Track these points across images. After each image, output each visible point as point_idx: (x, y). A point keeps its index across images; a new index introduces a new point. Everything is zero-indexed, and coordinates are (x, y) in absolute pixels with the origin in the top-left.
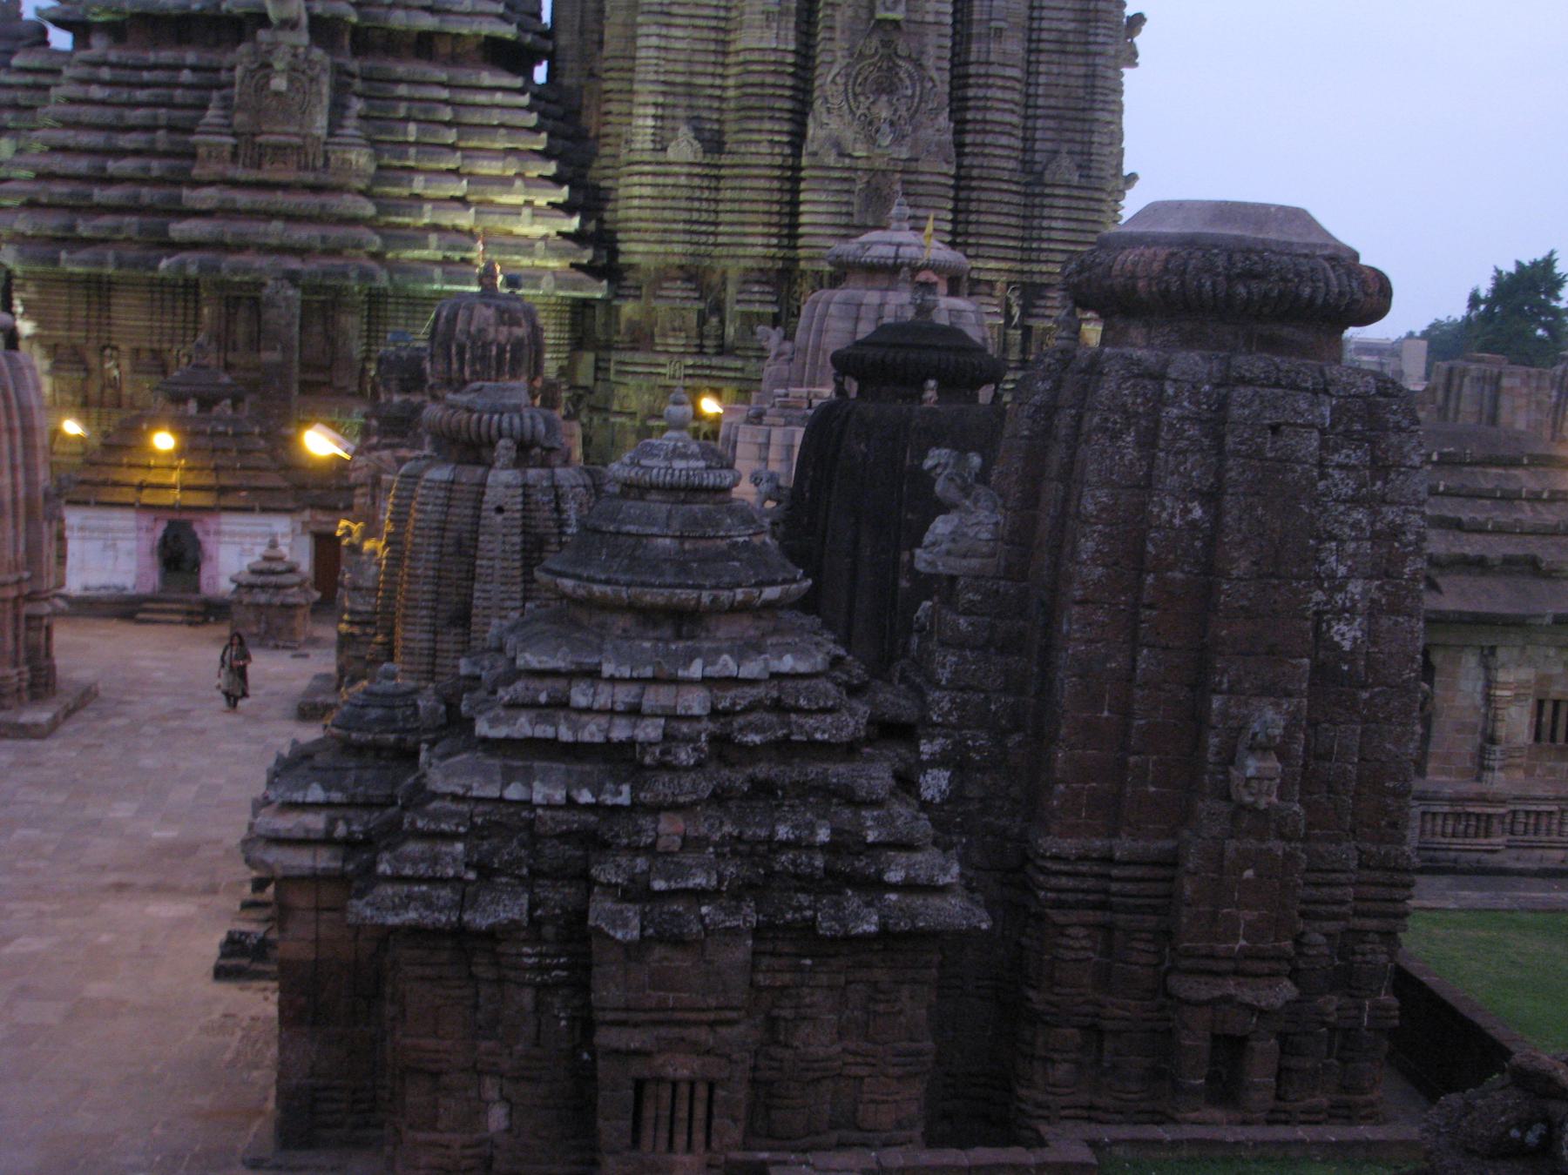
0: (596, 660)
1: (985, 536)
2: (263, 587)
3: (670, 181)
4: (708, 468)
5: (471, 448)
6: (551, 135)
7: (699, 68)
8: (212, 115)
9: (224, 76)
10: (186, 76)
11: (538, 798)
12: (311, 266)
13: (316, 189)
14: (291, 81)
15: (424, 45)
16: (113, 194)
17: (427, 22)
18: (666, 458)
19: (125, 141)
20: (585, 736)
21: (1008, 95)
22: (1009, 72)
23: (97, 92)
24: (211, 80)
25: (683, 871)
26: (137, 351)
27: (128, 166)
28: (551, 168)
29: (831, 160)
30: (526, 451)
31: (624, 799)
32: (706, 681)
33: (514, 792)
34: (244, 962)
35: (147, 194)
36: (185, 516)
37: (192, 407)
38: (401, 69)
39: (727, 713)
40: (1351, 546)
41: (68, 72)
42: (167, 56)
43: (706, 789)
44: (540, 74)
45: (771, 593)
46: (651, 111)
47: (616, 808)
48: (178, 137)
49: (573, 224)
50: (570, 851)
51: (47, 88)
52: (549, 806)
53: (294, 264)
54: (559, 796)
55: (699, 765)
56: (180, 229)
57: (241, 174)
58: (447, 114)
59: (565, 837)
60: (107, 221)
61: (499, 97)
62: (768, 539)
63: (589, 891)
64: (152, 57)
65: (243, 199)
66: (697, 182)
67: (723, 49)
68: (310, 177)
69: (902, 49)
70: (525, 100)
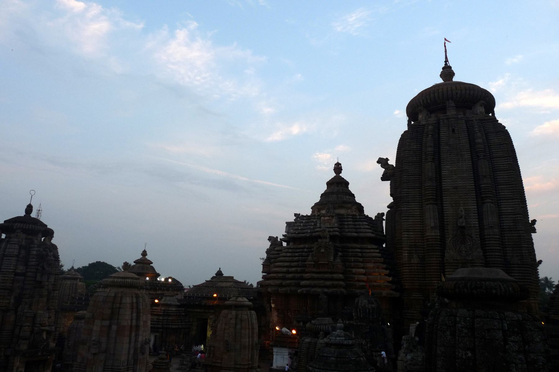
1: (420, 360)
3: (413, 268)
4: (345, 339)
7: (417, 241)
8: (310, 258)
9: (312, 249)
10: (305, 250)
12: (330, 290)
13: (331, 273)
15: (356, 240)
16: (290, 276)
17: (355, 234)
18: (336, 337)
19: (293, 264)
21: (496, 242)
22: (496, 237)
23: (289, 254)
27: (293, 269)
28: (385, 266)
35: (298, 275)
38: (350, 245)
40: (520, 366)
41: (283, 251)
42: (302, 246)
44: (384, 246)
46: (406, 252)
49: (390, 279)
53: (326, 290)
56: (303, 283)
58: (360, 254)
60: (288, 282)
61: (372, 251)
62: (362, 359)
65: (315, 276)
66: (419, 268)
68: (330, 270)
70: (378, 251)
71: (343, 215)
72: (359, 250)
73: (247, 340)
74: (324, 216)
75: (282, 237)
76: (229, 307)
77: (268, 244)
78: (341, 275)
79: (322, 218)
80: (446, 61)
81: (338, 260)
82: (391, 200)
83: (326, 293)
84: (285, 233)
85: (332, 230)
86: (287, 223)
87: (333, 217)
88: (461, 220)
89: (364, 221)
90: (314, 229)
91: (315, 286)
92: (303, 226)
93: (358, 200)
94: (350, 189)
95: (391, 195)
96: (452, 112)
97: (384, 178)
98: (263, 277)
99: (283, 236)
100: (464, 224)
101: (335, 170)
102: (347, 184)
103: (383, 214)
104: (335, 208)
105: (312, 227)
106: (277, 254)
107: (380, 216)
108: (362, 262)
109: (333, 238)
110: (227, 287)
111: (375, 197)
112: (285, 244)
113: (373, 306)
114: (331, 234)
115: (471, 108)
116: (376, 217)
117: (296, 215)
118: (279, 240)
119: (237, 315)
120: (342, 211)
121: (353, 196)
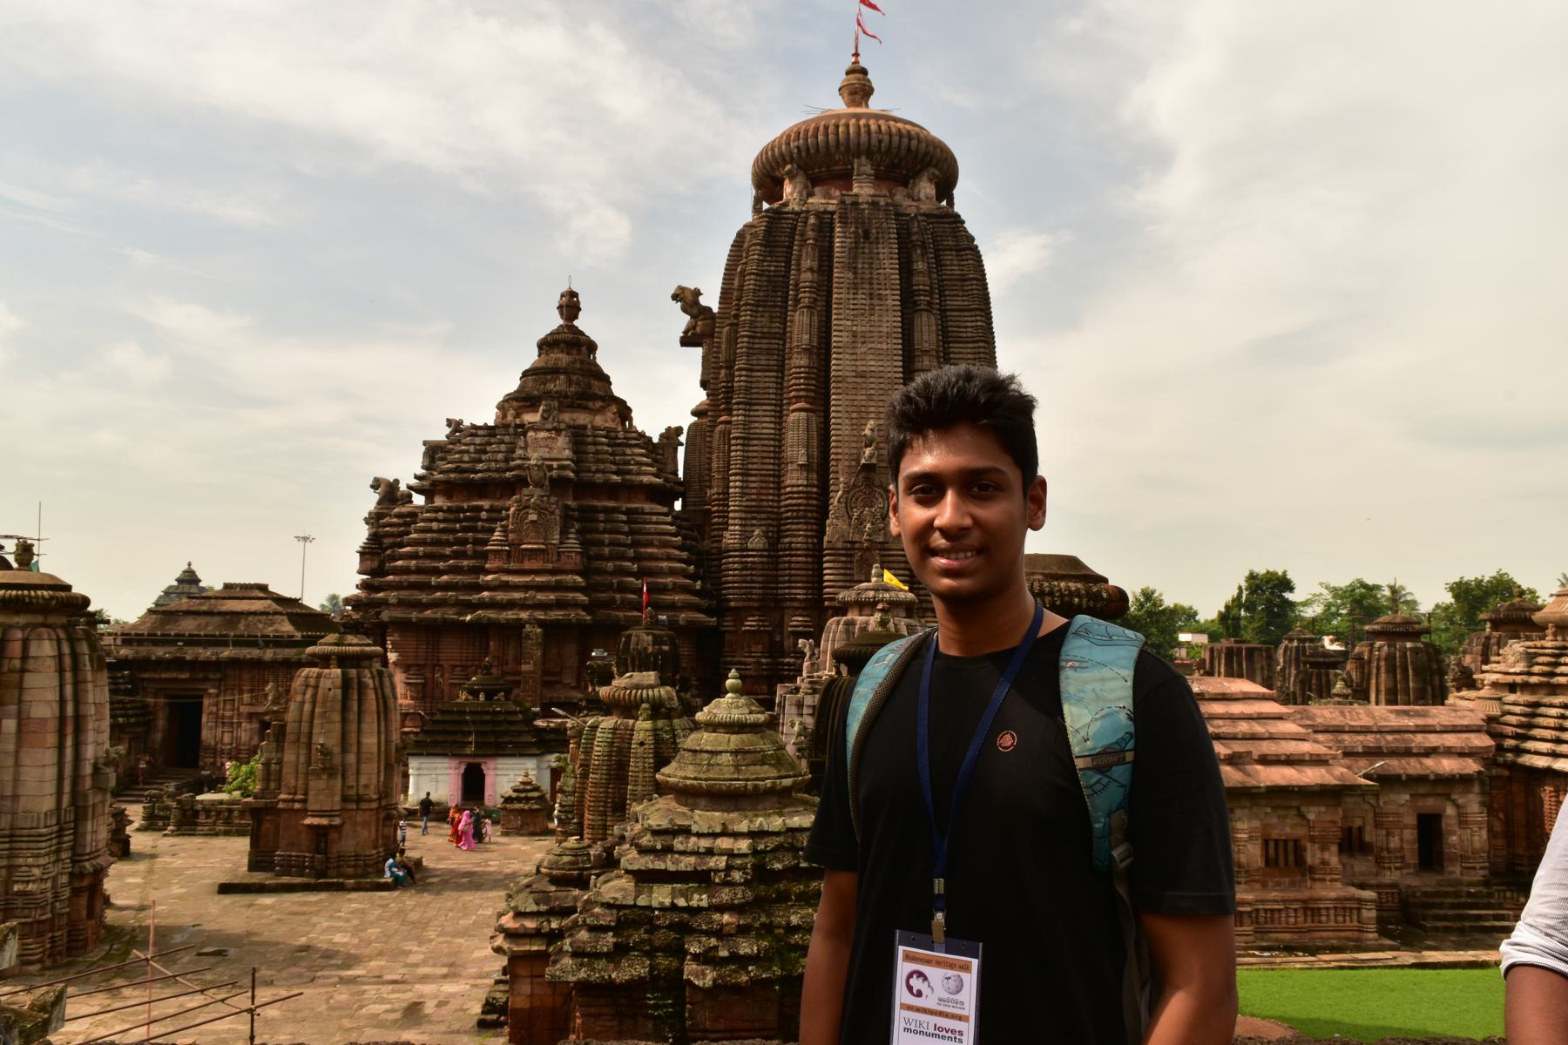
0: (687, 823)
2: (519, 800)
5: (627, 708)
6: (685, 538)
8: (497, 535)
11: (655, 904)
13: (553, 572)
14: (539, 514)
15: (612, 490)
20: (682, 867)
23: (435, 525)
24: (496, 514)
25: (737, 945)
26: (454, 667)
29: (840, 545)
30: (657, 710)
31: (704, 904)
32: (751, 834)
33: (642, 901)
34: (495, 1017)
36: (477, 760)
37: (482, 697)
39: (763, 852)
43: (749, 895)
44: (678, 505)
45: (787, 782)
47: (699, 909)
48: (479, 548)
50: (673, 935)
51: (407, 524)
52: (663, 909)
53: (540, 615)
54: (667, 902)
55: (747, 883)
57: (513, 566)
58: (626, 528)
59: (671, 927)
61: (654, 518)
63: (683, 960)
64: (465, 505)
67: (779, 486)
68: (550, 566)
69: (877, 482)
70: (669, 519)
71: (584, 427)
72: (624, 517)
73: (375, 740)
74: (536, 430)
75: (414, 482)
76: (323, 660)
77: (371, 501)
78: (579, 579)
79: (531, 434)
80: (856, 55)
81: (573, 541)
82: (701, 396)
83: (541, 623)
84: (421, 472)
85: (555, 464)
86: (425, 443)
87: (558, 431)
88: (868, 451)
89: (636, 446)
90: (507, 460)
91: (511, 605)
92: (476, 452)
93: (618, 390)
94: (598, 361)
95: (704, 384)
96: (862, 190)
97: (686, 341)
98: (364, 586)
99: (416, 477)
100: (874, 461)
101: (560, 307)
102: (592, 347)
103: (679, 430)
104: (561, 410)
105: (500, 456)
106: (399, 525)
107: (671, 435)
108: (630, 546)
109: (558, 485)
110: (254, 613)
111: (661, 390)
112: (419, 500)
113: (666, 648)
114: (554, 473)
115: (906, 185)
116: (662, 436)
117: (449, 423)
118: (403, 487)
119: (346, 683)
120: (582, 418)
121: (606, 380)
